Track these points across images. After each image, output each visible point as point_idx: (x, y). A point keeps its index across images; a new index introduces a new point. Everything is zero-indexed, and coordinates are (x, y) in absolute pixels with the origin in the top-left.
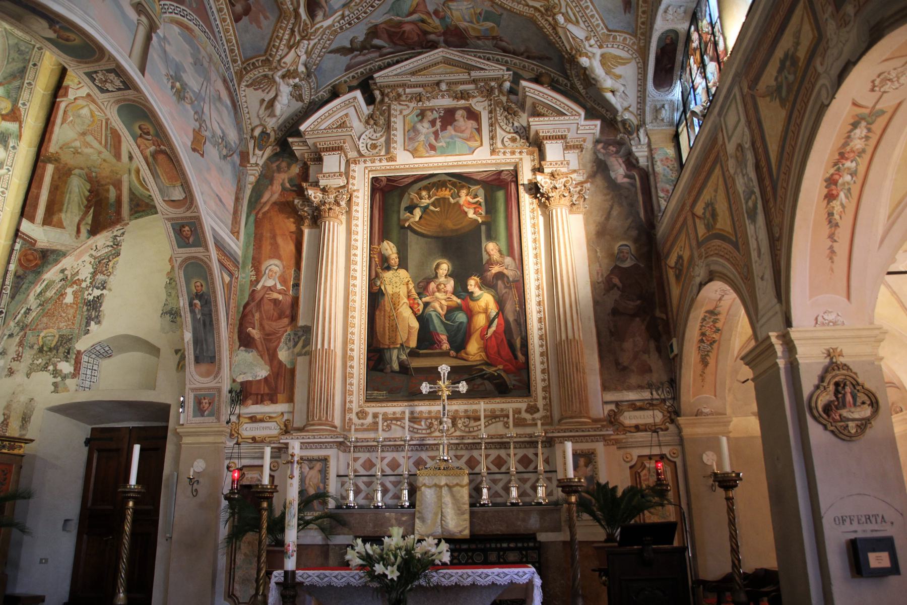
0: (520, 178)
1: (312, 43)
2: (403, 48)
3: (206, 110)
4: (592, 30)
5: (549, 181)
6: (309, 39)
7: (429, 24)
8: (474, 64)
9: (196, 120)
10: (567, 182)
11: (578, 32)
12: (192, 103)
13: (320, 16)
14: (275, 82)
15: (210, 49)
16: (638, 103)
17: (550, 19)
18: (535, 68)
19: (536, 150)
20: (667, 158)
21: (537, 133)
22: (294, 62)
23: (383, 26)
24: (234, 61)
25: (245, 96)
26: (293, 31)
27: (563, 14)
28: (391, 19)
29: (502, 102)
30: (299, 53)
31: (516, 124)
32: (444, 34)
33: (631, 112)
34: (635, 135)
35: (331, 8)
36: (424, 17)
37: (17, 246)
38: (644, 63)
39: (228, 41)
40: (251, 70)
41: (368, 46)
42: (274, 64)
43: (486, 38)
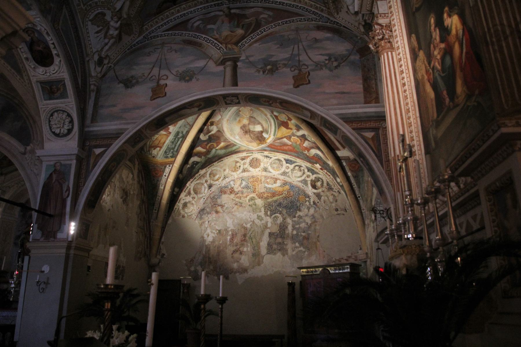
3: (303, 58)
9: (295, 70)
12: (285, 65)
15: (293, 26)
25: (343, 19)
37: (344, 164)
39: (311, 6)
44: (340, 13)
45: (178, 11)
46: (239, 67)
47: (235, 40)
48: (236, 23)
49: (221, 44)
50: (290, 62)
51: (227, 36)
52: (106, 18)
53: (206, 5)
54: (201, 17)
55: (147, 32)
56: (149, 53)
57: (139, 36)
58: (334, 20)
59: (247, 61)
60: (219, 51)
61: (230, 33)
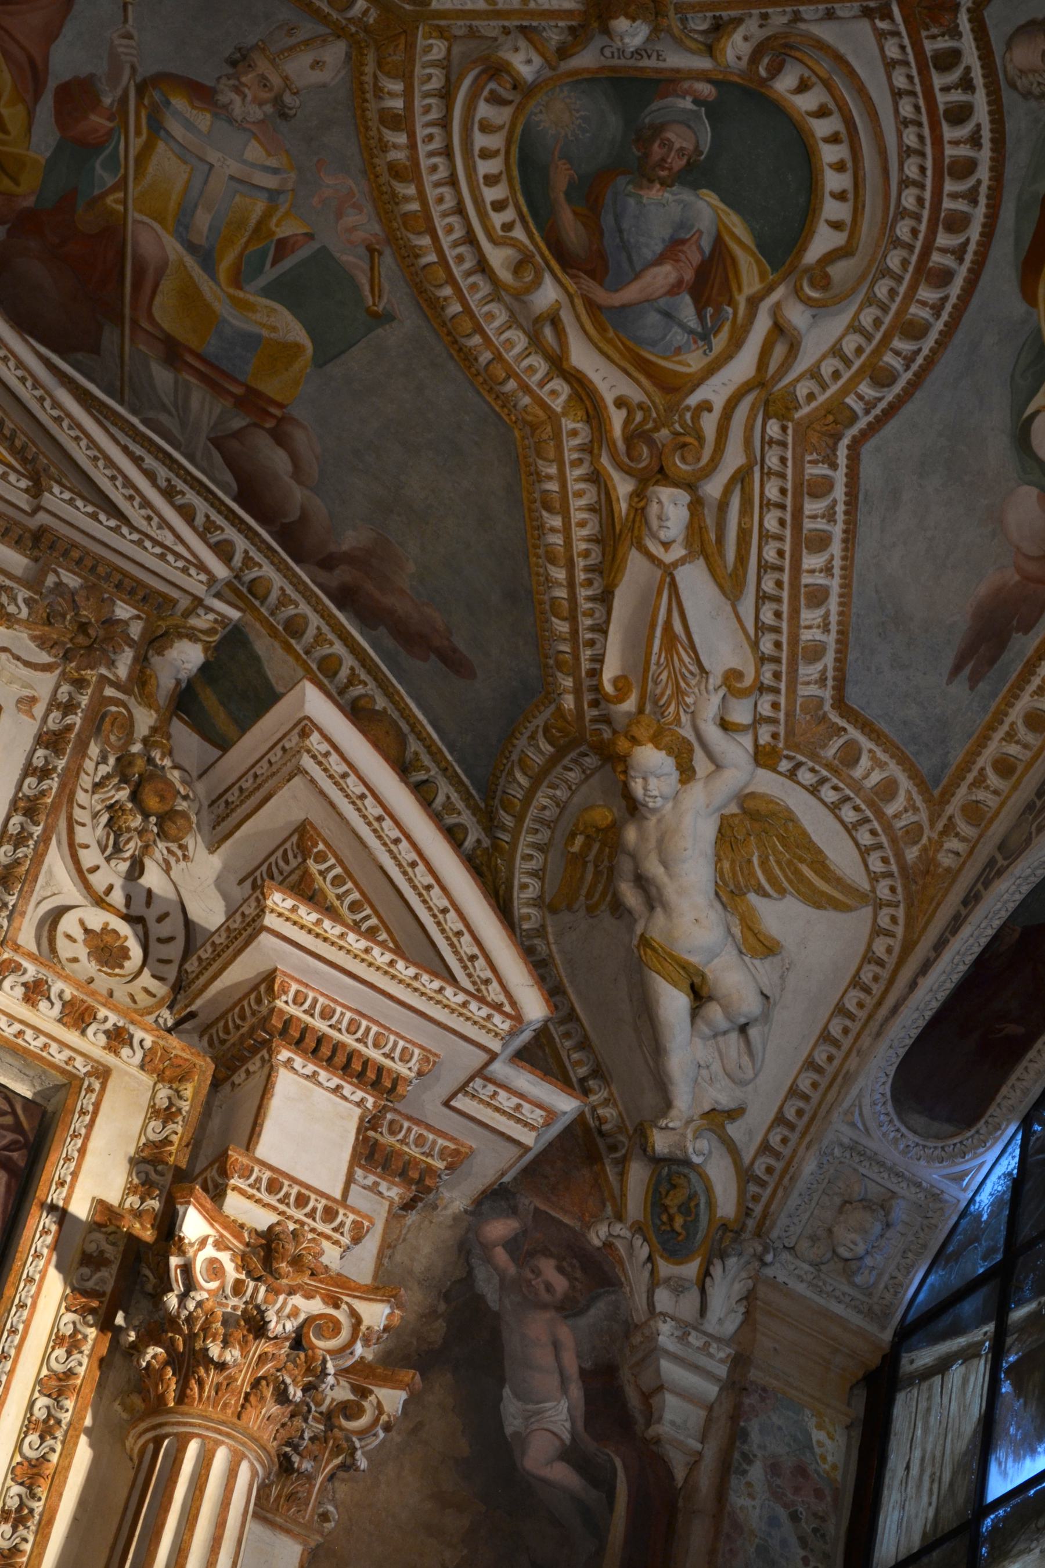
0: (56, 1168)
4: (778, 655)
5: (232, 1272)
8: (81, 455)
10: (328, 1326)
11: (717, 632)
16: (780, 1119)
17: (623, 487)
18: (349, 661)
19: (206, 1066)
20: (801, 1471)
21: (269, 977)
27: (696, 505)
29: (128, 725)
31: (153, 878)
33: (732, 1148)
34: (691, 1269)
38: (908, 947)
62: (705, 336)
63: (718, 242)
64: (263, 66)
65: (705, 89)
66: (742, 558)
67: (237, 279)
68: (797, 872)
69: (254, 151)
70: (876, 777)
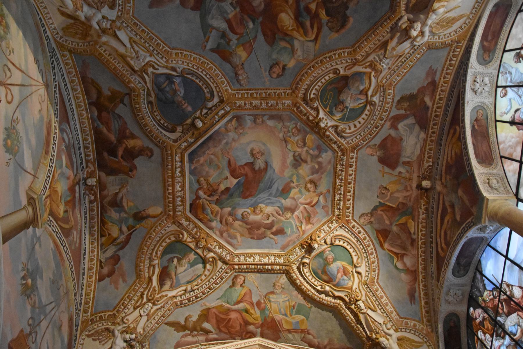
1: (155, 308)
2: (228, 336)
3: (44, 324)
6: (154, 304)
7: (250, 314)
11: (378, 317)
13: (168, 284)
14: (114, 335)
15: (70, 284)
22: (136, 321)
23: (214, 310)
24: (86, 312)
26: (142, 294)
28: (222, 305)
30: (142, 313)
32: (262, 326)
35: (178, 280)
36: (248, 307)
39: (87, 294)
40: (97, 321)
41: (198, 328)
42: (119, 320)
43: (296, 331)
44: (91, 339)
45: (78, 106)
46: (27, 230)
47: (54, 206)
48: (69, 199)
49: (50, 188)
50: (37, 310)
51: (57, 191)
52: (106, 6)
53: (81, 145)
54: (71, 141)
55: (58, 55)
56: (38, 60)
57: (55, 41)
58: (78, 332)
59: (35, 242)
60: (42, 188)
61: (60, 195)
62: (350, 280)
63: (343, 267)
64: (277, 284)
65: (329, 249)
66: (374, 306)
67: (291, 316)
68: (412, 345)
69: (283, 296)
70: (412, 324)
